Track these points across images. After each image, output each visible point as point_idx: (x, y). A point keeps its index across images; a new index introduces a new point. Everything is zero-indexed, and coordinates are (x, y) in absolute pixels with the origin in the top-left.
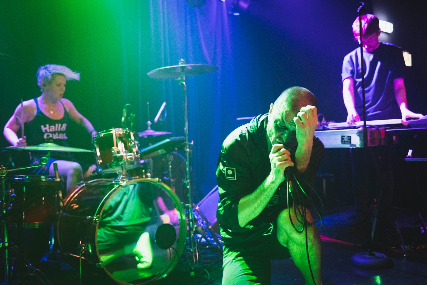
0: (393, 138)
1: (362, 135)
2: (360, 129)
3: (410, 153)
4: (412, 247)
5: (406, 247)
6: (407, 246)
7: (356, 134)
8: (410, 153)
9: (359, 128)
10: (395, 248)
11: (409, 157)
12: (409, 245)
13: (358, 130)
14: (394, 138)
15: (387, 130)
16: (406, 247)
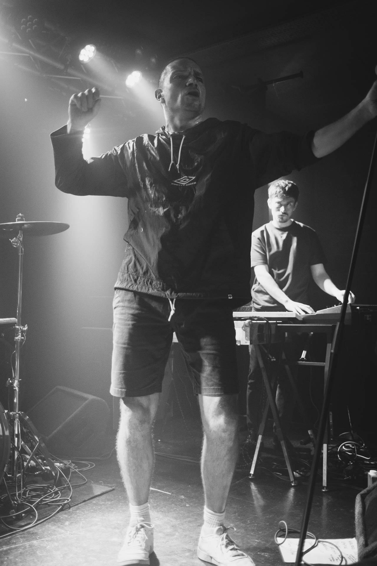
0: (285, 334)
1: (248, 329)
2: (247, 321)
3: (304, 354)
4: (301, 473)
5: (294, 473)
6: (296, 472)
7: (241, 328)
8: (304, 354)
9: (245, 320)
10: (281, 474)
11: (303, 359)
12: (298, 471)
13: (244, 323)
14: (286, 334)
15: (278, 325)
16: (294, 473)
